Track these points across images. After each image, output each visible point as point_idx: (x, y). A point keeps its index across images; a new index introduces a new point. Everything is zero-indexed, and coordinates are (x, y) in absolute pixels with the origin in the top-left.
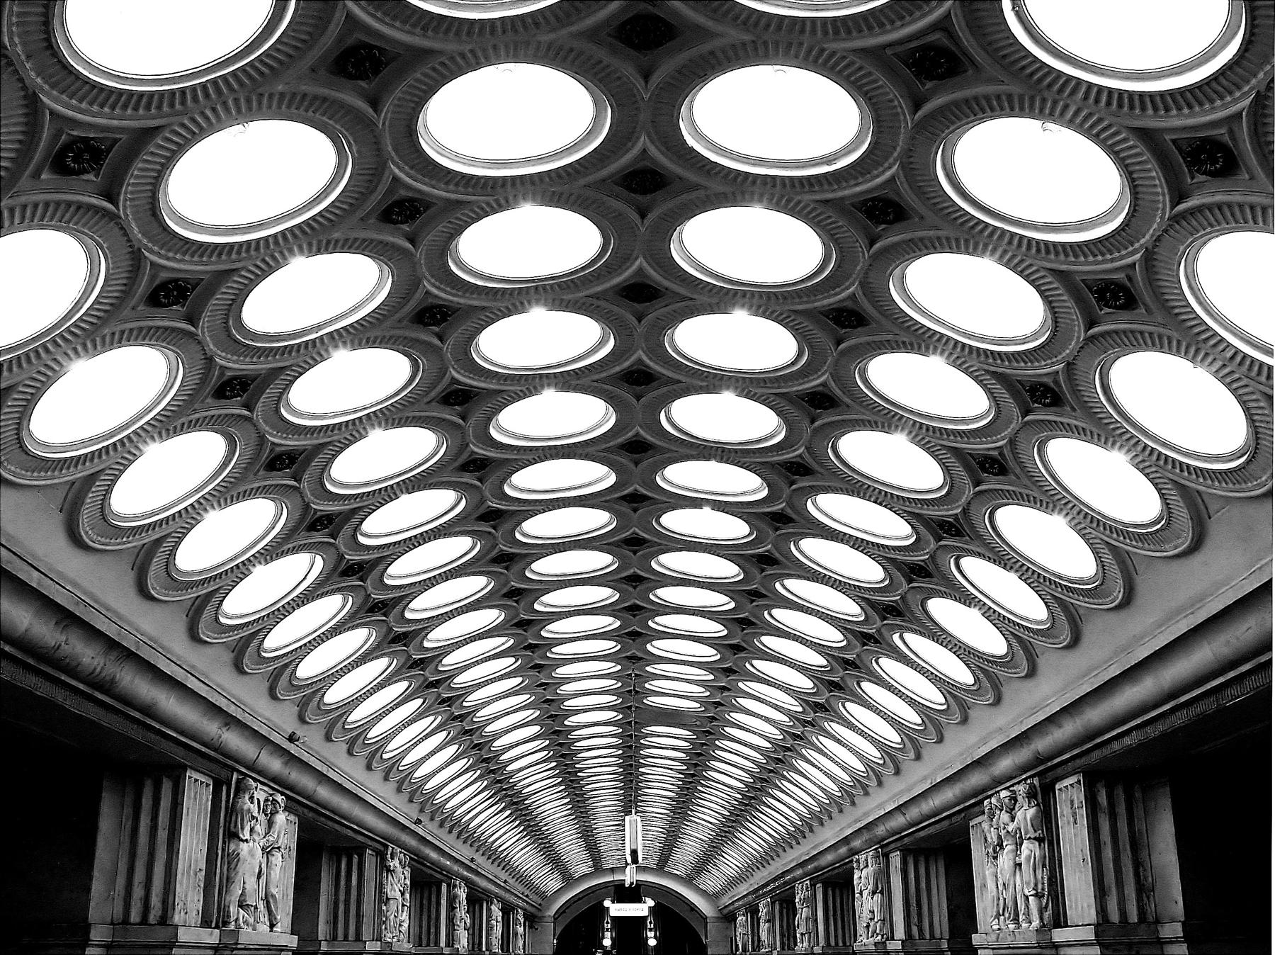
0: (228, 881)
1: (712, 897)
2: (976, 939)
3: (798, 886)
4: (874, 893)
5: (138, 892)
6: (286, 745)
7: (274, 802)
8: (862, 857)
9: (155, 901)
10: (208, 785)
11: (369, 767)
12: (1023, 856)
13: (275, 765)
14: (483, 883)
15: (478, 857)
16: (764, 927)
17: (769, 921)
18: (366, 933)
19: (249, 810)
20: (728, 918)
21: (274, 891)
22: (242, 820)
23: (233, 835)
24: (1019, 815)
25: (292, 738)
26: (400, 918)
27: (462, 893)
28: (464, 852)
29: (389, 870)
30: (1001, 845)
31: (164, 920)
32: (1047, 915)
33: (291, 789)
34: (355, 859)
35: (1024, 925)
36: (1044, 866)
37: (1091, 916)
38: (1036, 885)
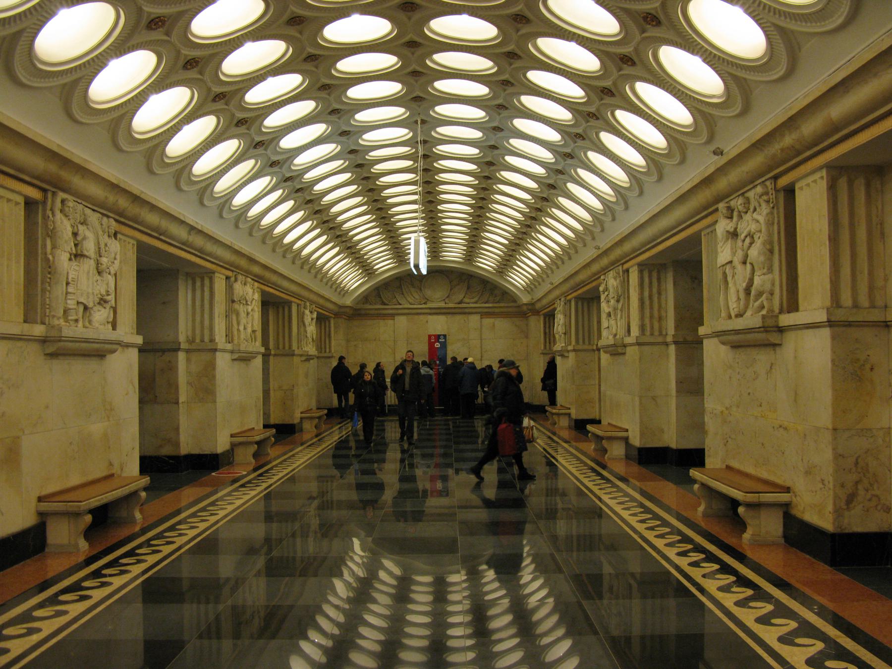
2: (702, 331)
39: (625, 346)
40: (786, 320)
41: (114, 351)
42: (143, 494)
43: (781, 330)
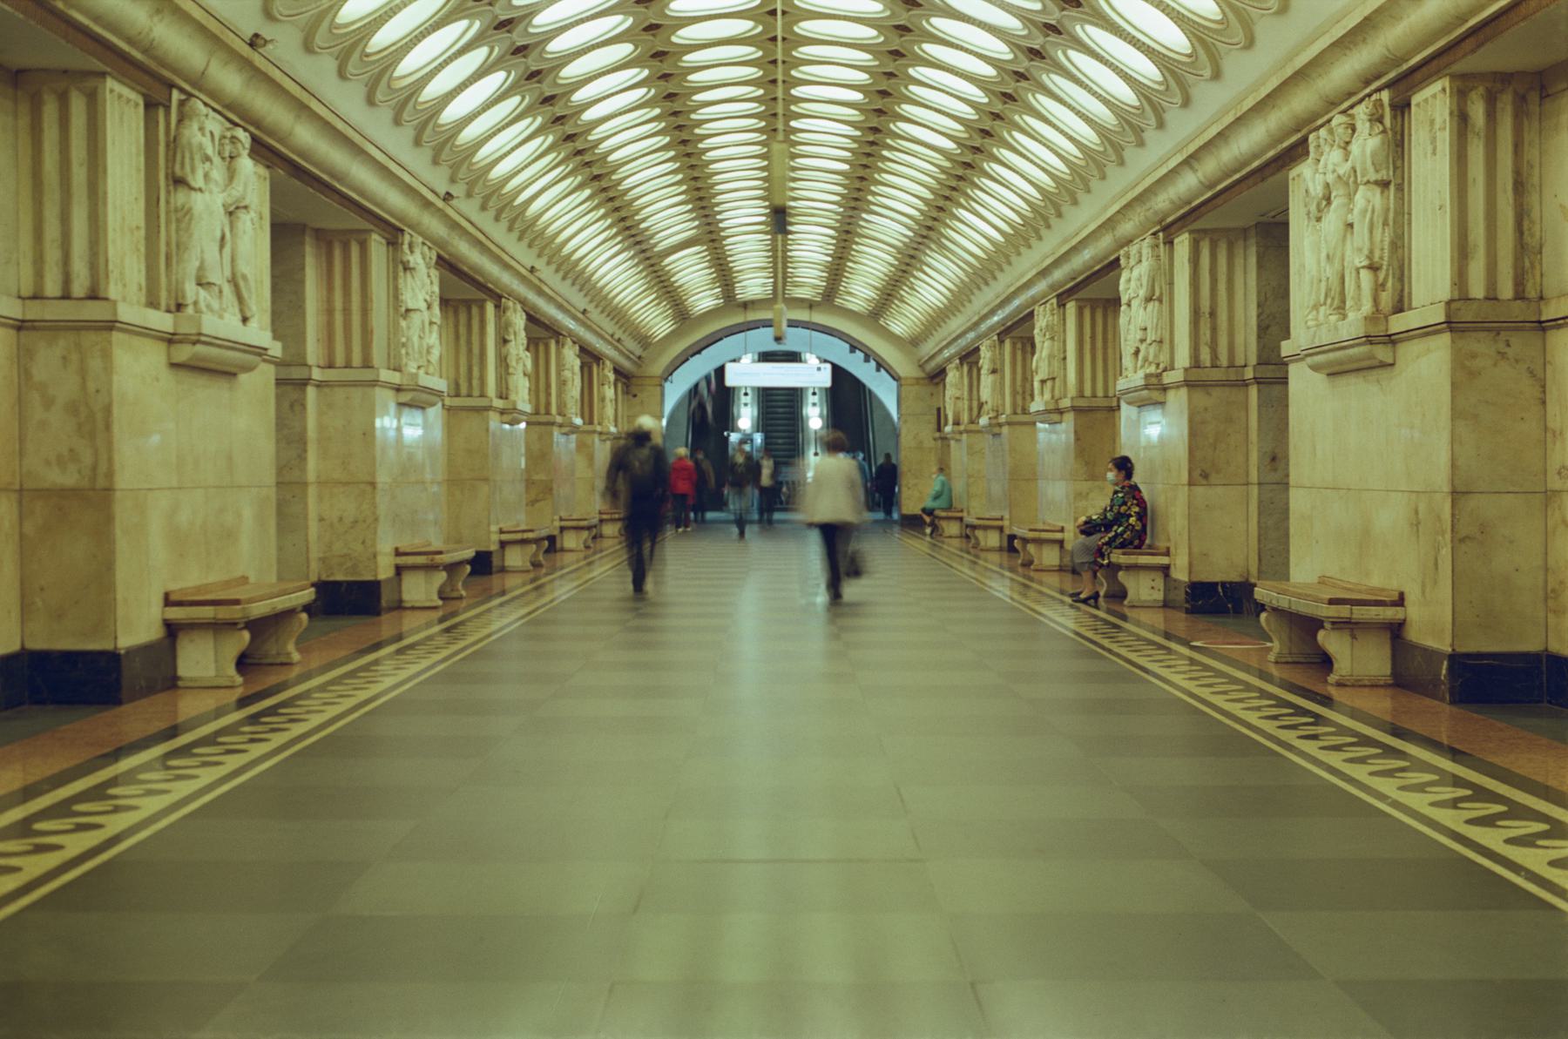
0: (178, 249)
1: (915, 341)
2: (1287, 348)
3: (1039, 310)
4: (1149, 299)
5: (52, 255)
6: (246, 50)
7: (234, 139)
8: (1133, 249)
9: (80, 268)
10: (137, 105)
11: (371, 101)
12: (1356, 211)
13: (231, 81)
14: (551, 311)
15: (540, 264)
16: (987, 381)
17: (994, 371)
18: (378, 354)
19: (201, 147)
20: (937, 377)
21: (243, 268)
22: (192, 159)
23: (179, 182)
24: (1355, 148)
25: (255, 42)
26: (425, 340)
27: (518, 320)
28: (523, 255)
29: (407, 268)
30: (1328, 199)
31: (94, 295)
32: (1386, 298)
33: (258, 125)
34: (355, 250)
35: (1351, 316)
36: (1385, 223)
37: (1444, 291)
38: (1371, 252)
39: (1165, 389)
40: (1398, 324)
41: (249, 368)
42: (304, 616)
43: (1391, 340)
